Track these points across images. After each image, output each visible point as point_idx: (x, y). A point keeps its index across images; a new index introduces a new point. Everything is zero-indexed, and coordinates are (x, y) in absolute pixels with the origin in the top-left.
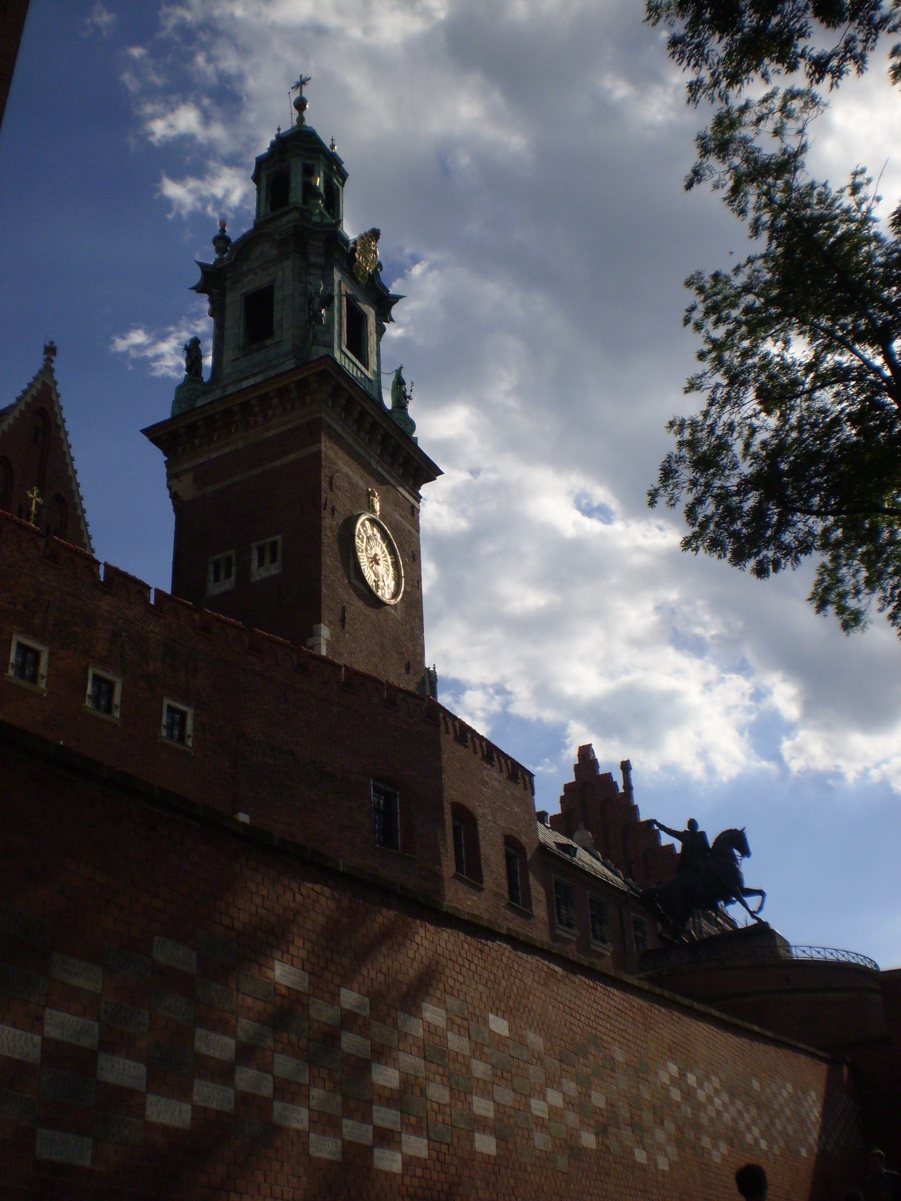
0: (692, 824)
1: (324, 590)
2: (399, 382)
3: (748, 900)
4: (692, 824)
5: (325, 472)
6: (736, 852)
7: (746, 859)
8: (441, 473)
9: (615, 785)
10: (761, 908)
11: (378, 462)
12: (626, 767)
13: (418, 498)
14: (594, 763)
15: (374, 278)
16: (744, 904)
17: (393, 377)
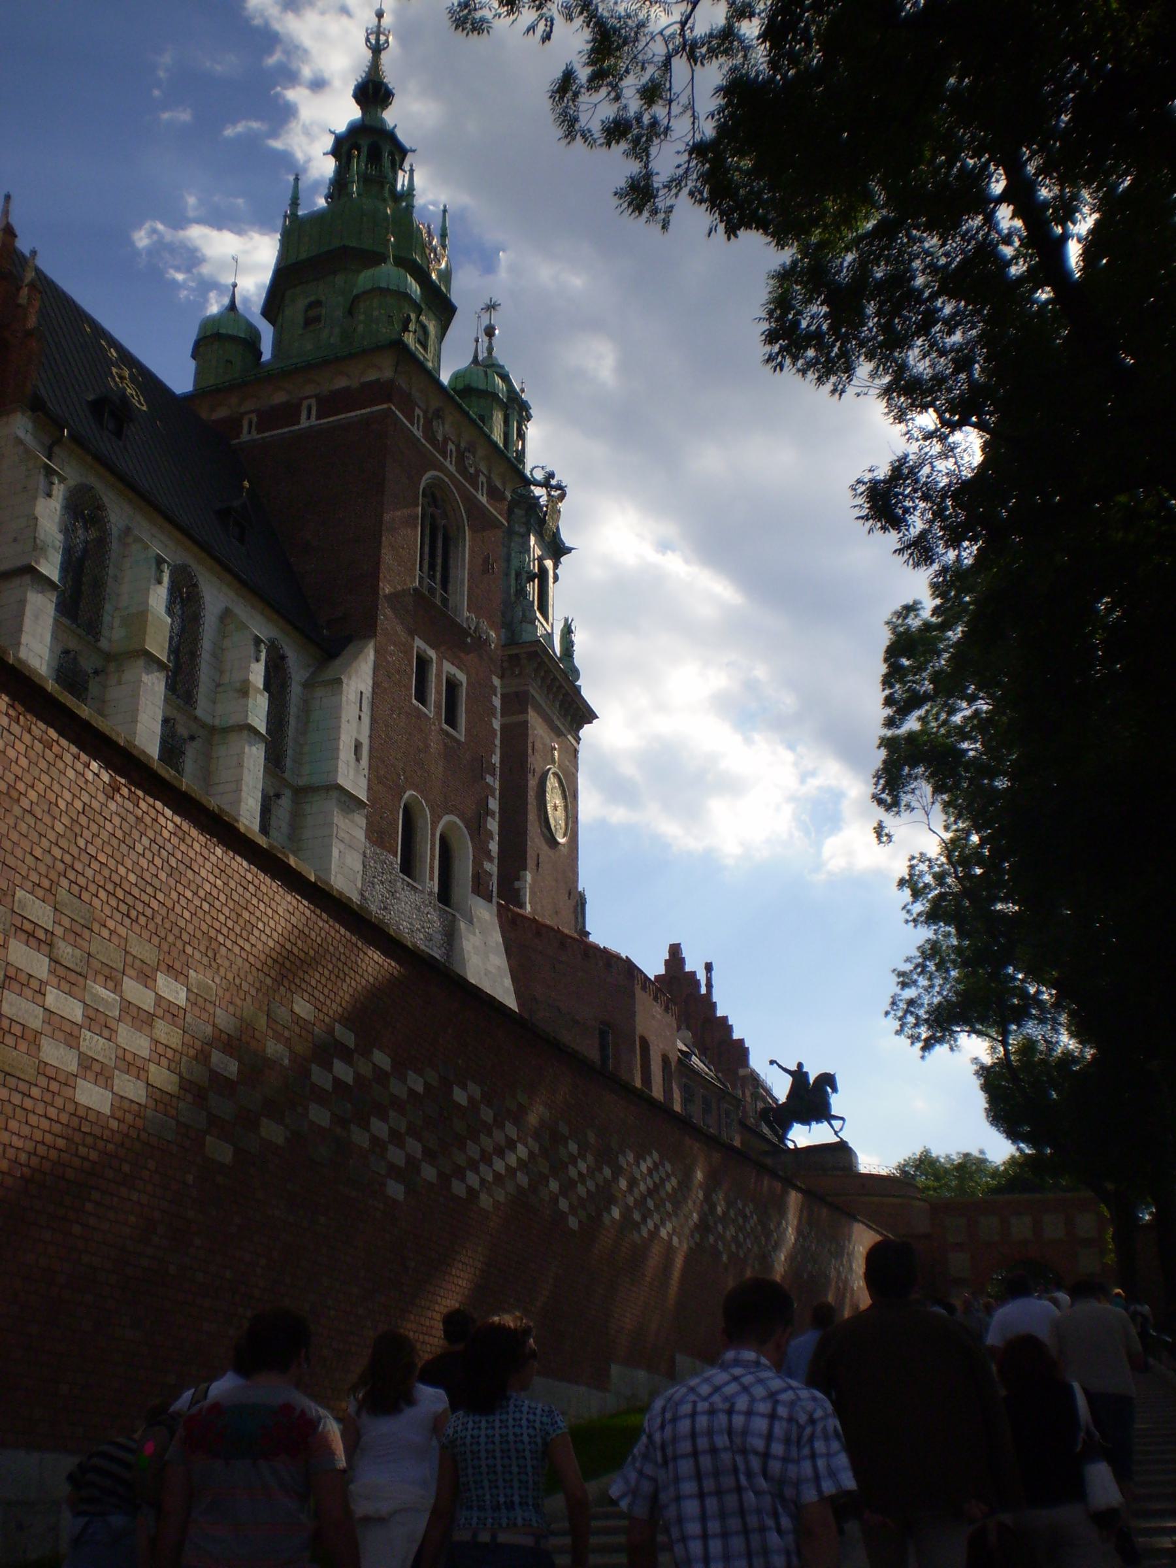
0: (800, 1065)
1: (529, 843)
2: (567, 631)
3: (833, 1122)
4: (800, 1065)
5: (530, 740)
6: (829, 1090)
7: (834, 1095)
8: (597, 717)
9: (698, 983)
10: (841, 1129)
11: (558, 719)
12: (709, 967)
13: (578, 740)
14: (682, 961)
15: (556, 535)
16: (832, 1126)
17: (563, 621)
